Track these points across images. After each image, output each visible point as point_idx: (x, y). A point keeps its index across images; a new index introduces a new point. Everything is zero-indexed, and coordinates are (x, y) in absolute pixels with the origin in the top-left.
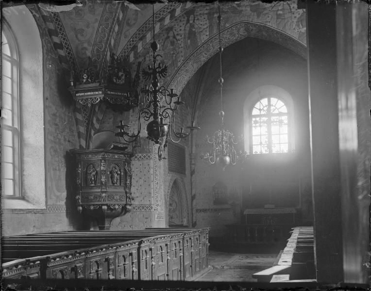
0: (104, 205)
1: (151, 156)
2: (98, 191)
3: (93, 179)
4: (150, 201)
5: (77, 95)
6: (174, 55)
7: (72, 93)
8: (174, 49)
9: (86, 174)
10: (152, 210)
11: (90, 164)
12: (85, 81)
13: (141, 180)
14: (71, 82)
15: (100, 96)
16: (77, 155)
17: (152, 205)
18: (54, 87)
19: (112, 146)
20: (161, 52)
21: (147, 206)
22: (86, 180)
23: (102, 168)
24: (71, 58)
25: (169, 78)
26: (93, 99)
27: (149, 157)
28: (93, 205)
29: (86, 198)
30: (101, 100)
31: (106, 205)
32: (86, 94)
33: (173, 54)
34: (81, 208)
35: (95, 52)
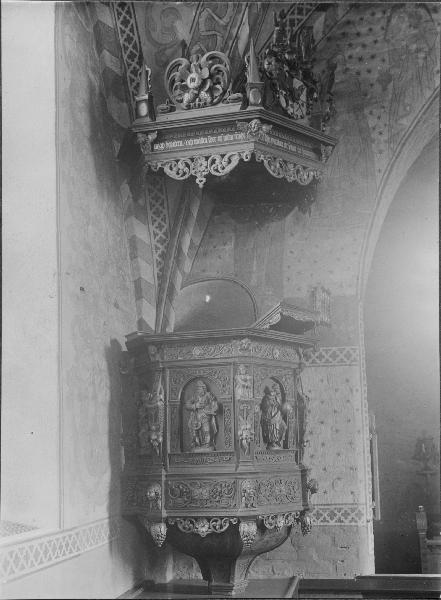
0: (246, 519)
1: (354, 355)
2: (225, 470)
3: (206, 429)
4: (352, 493)
5: (156, 147)
6: (422, 55)
7: (141, 138)
8: (417, 38)
9: (181, 411)
10: (360, 524)
11: (195, 379)
12: (187, 97)
13: (323, 427)
14: (141, 101)
15: (238, 148)
16: (152, 349)
17: (360, 508)
18: (83, 118)
19: (276, 319)
20: (378, 45)
21: (345, 508)
22: (180, 433)
23: (239, 392)
24: (129, 39)
25: (405, 122)
26: (214, 161)
27: (348, 356)
28: (209, 519)
29: (180, 495)
30: (241, 160)
31: (254, 518)
32: (190, 142)
33: (418, 50)
34: (162, 529)
35: (202, 27)
